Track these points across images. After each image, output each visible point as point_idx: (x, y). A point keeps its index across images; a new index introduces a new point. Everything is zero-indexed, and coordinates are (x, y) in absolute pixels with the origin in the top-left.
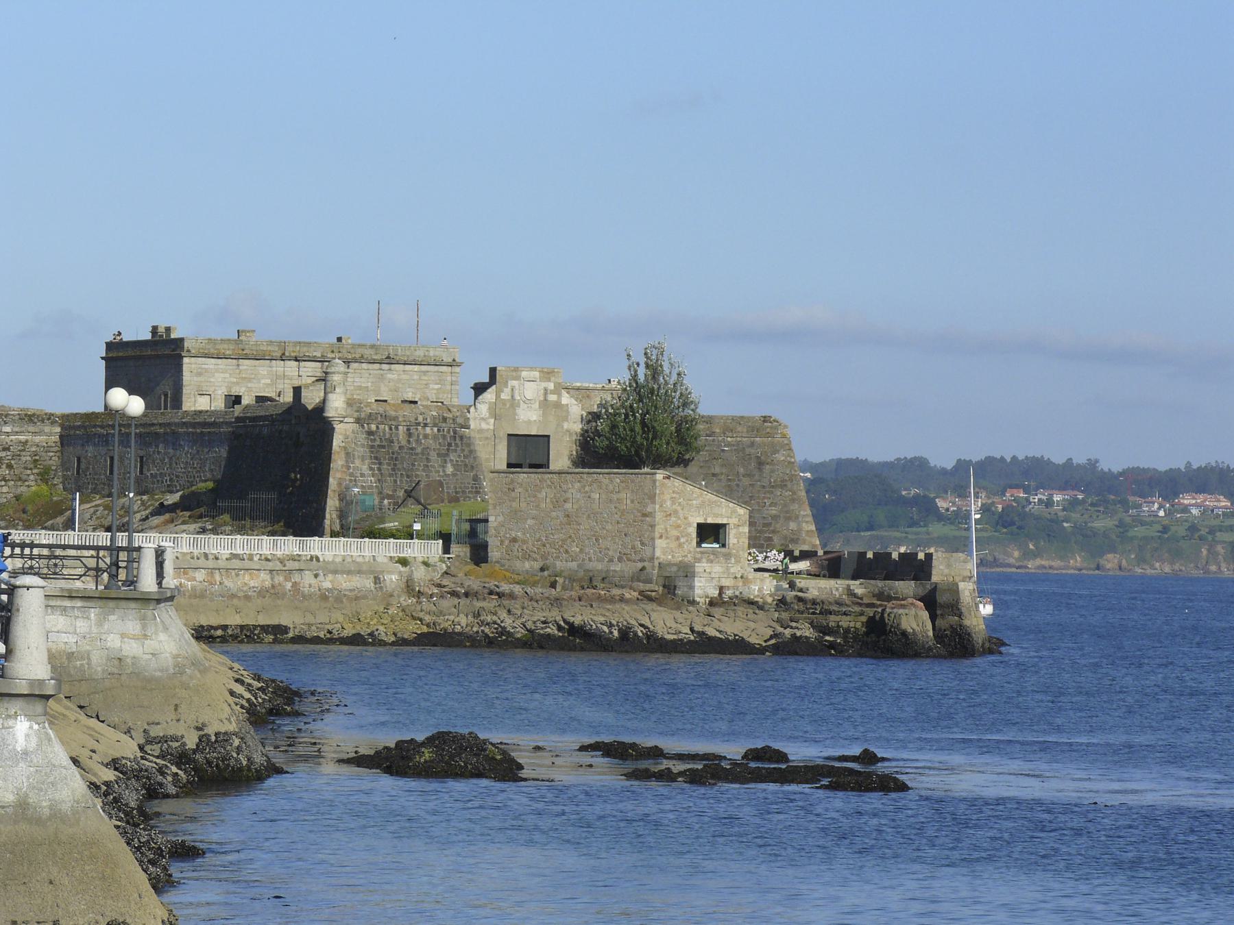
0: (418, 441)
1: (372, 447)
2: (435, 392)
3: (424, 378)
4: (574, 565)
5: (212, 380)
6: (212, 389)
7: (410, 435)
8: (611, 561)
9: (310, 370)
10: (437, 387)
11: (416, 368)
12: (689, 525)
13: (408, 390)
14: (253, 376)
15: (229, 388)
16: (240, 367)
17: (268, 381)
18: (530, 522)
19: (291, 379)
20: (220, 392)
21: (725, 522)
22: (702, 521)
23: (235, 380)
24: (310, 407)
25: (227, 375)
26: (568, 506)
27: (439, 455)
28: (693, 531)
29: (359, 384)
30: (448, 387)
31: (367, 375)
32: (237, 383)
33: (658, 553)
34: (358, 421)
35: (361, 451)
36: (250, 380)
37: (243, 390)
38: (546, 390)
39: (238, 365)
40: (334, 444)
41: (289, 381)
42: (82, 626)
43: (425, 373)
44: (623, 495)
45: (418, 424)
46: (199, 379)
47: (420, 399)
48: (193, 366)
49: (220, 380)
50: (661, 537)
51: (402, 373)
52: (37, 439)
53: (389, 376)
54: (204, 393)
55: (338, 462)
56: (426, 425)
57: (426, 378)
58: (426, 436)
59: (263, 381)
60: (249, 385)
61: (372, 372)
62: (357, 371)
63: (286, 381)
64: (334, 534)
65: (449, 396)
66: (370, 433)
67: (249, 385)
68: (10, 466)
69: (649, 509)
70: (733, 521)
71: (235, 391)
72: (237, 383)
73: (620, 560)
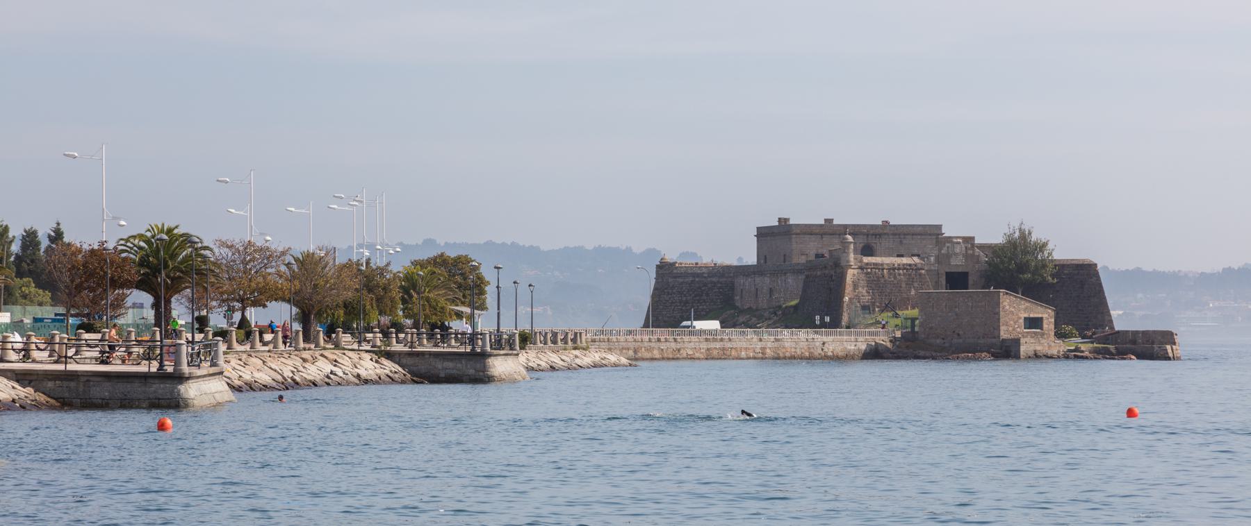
0: (895, 278)
1: (869, 281)
4: (961, 341)
5: (809, 246)
7: (891, 274)
8: (979, 338)
10: (931, 246)
11: (919, 237)
12: (1020, 318)
18: (939, 318)
21: (1040, 316)
22: (1026, 315)
23: (820, 246)
24: (756, 263)
26: (957, 309)
27: (906, 284)
28: (1022, 321)
33: (1002, 333)
34: (861, 268)
35: (862, 283)
38: (966, 248)
40: (848, 279)
42: (459, 365)
44: (983, 303)
45: (895, 269)
50: (1003, 325)
52: (721, 280)
55: (849, 289)
56: (899, 269)
58: (900, 274)
64: (848, 327)
66: (868, 273)
68: (707, 295)
69: (997, 310)
70: (1045, 316)
71: (820, 251)
72: (822, 248)
73: (983, 338)
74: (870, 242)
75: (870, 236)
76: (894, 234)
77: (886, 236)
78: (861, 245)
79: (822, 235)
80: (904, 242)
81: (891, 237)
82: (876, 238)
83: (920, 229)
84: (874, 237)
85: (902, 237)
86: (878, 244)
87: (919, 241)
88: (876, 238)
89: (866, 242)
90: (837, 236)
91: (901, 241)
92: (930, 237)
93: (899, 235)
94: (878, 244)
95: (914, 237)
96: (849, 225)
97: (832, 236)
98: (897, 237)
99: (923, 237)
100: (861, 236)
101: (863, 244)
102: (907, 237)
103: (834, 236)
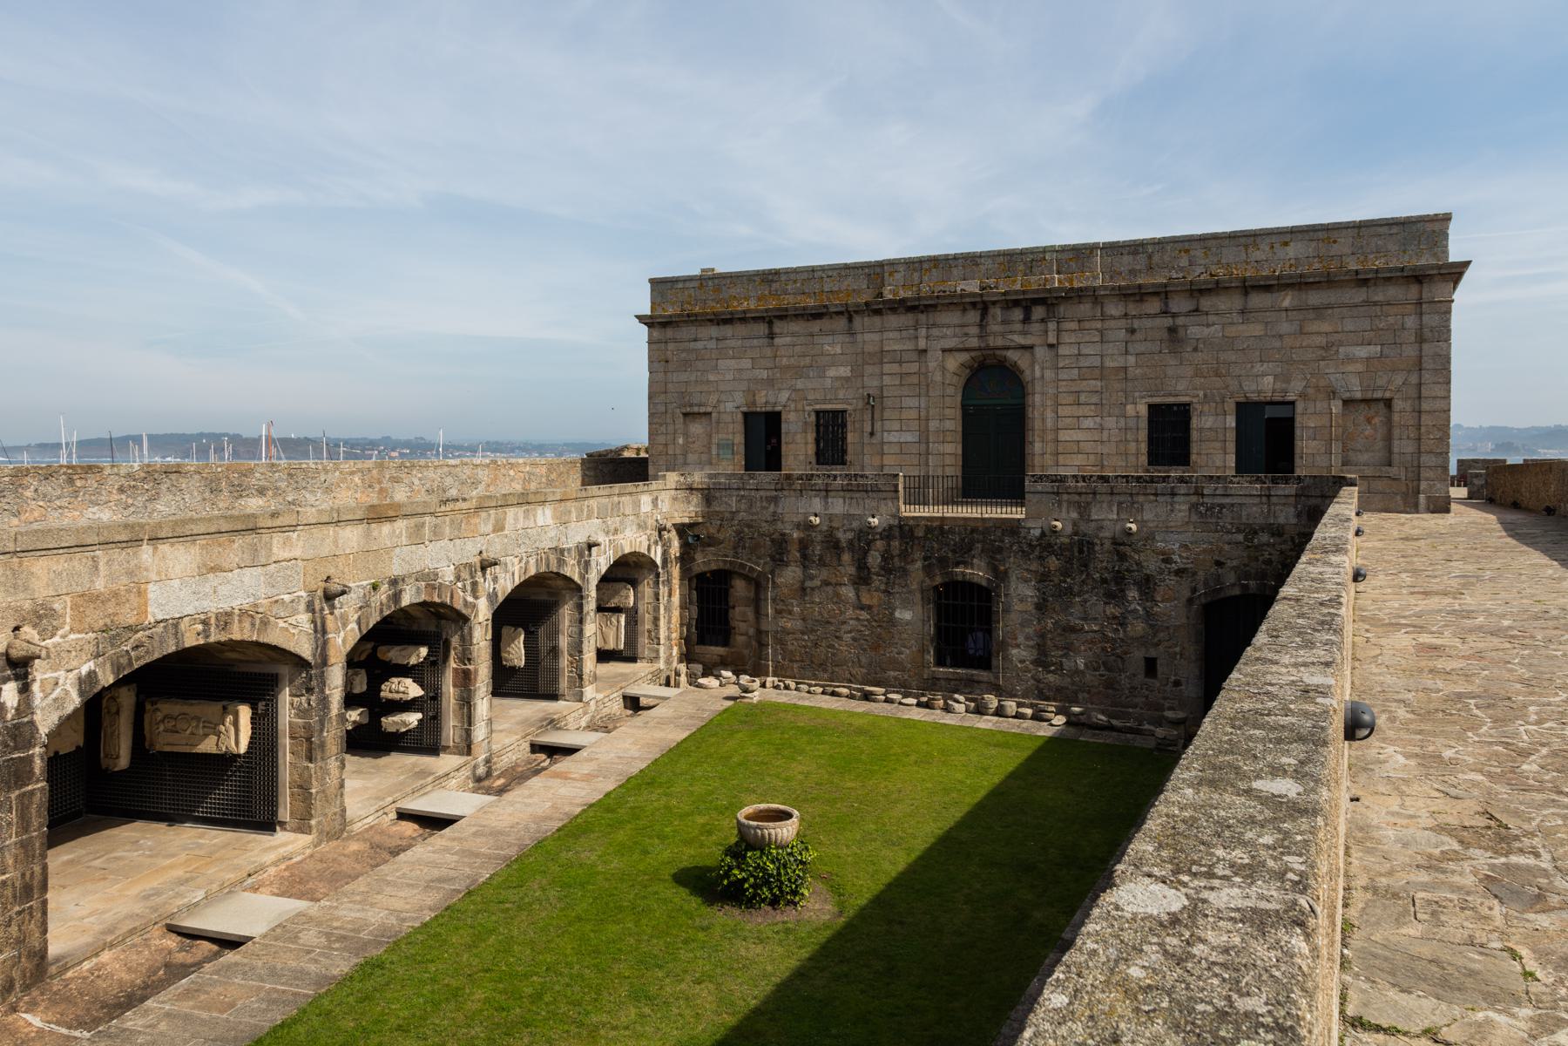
2: (1360, 367)
3: (1314, 327)
5: (712, 378)
6: (713, 399)
9: (949, 332)
10: (1362, 352)
11: (1287, 300)
13: (1259, 368)
14: (808, 360)
15: (750, 393)
16: (777, 341)
17: (845, 371)
19: (900, 362)
20: (730, 406)
23: (764, 374)
25: (746, 363)
29: (1096, 362)
30: (1410, 351)
31: (1122, 334)
32: (770, 382)
36: (799, 372)
37: (784, 396)
39: (771, 336)
41: (895, 368)
43: (1319, 311)
46: (684, 377)
47: (1303, 395)
48: (671, 346)
49: (729, 376)
51: (1237, 318)
53: (1195, 331)
54: (696, 409)
57: (1325, 327)
59: (832, 372)
60: (800, 384)
61: (1136, 324)
62: (1087, 325)
63: (887, 368)
65: (1414, 379)
67: (800, 384)
72: (770, 382)
74: (992, 341)
75: (997, 312)
76: (1138, 294)
77: (1085, 308)
78: (953, 363)
79: (770, 323)
80: (1195, 331)
81: (1114, 309)
82: (1027, 319)
83: (1294, 250)
84: (1018, 314)
85: (1180, 304)
86: (1041, 352)
87: (1285, 327)
88: (1027, 319)
89: (974, 342)
90: (842, 323)
91: (1172, 330)
92: (1360, 295)
93: (1163, 293)
94: (1041, 352)
95: (1257, 300)
96: (892, 263)
97: (816, 326)
98: (1153, 306)
99: (1315, 298)
100: (953, 317)
101: (964, 357)
102: (1206, 303)
103: (824, 324)
